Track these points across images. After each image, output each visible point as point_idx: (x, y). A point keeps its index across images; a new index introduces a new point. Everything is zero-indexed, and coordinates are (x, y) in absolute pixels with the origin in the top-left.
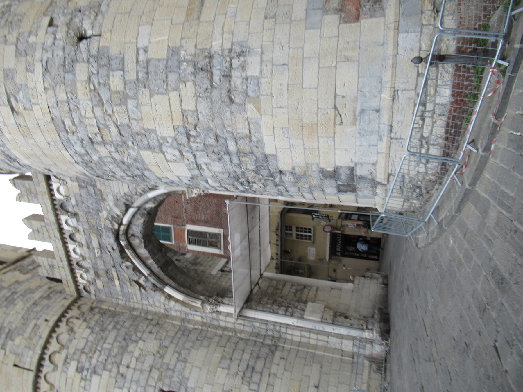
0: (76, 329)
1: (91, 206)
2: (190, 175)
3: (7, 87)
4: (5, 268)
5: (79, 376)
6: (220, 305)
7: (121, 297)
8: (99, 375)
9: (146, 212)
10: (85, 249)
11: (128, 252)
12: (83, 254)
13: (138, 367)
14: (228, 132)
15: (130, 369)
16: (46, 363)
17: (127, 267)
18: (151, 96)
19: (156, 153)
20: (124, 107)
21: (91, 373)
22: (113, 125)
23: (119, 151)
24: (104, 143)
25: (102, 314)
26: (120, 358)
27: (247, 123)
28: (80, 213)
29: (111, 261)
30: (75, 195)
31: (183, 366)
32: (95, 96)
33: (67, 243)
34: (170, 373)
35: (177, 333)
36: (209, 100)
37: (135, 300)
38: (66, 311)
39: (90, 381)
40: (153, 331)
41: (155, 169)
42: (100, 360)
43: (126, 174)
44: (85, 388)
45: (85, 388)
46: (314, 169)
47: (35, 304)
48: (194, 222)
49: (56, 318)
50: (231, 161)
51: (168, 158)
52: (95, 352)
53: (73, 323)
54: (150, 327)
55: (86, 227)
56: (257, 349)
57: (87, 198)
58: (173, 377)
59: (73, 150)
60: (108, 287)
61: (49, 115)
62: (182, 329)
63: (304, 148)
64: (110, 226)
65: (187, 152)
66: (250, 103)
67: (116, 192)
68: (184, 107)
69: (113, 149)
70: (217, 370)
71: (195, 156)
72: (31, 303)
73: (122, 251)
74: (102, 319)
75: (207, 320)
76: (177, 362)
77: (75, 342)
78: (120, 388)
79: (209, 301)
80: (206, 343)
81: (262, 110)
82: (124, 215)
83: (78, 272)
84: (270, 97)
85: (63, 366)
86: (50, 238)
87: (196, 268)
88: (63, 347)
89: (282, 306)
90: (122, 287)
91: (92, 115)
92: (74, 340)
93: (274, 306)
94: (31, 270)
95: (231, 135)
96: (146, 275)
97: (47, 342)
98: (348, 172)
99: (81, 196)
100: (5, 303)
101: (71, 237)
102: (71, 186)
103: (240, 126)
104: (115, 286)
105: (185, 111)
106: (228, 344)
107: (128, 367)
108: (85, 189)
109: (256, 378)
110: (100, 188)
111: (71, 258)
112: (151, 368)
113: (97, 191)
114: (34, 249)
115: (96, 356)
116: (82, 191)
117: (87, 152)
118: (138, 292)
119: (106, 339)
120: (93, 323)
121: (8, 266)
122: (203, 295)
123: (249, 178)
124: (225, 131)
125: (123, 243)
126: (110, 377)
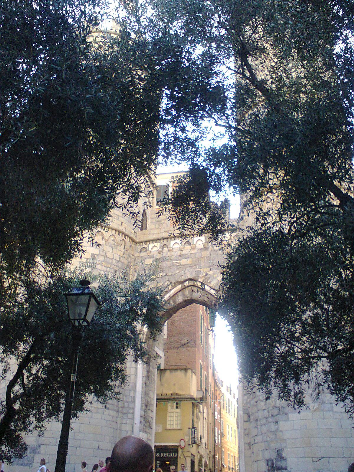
0: (119, 247)
10: (179, 253)
12: (174, 250)
29: (171, 273)
38: (128, 236)
46: (282, 444)
49: (124, 231)
55: (197, 256)
63: (295, 439)
73: (180, 283)
77: (110, 249)
83: (158, 244)
88: (107, 241)
98: (284, 466)
120: (123, 260)
125: (187, 283)
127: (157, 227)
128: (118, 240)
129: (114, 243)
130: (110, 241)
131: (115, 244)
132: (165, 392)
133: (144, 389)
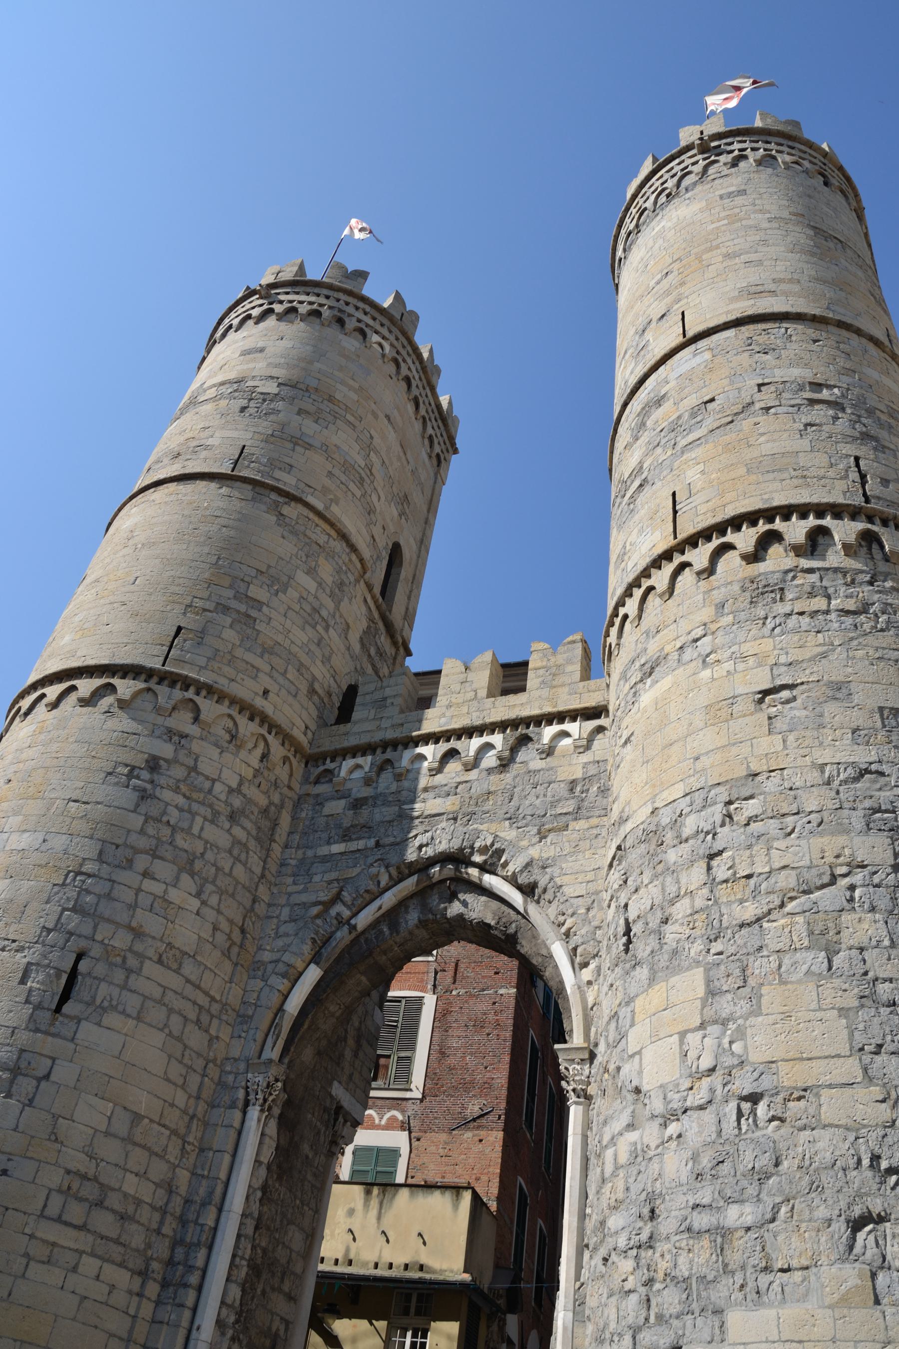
0: (243, 754)
1: (527, 802)
2: (645, 1088)
3: (811, 685)
4: (376, 602)
5: (139, 760)
6: (262, 1111)
7: (300, 852)
8: (137, 805)
9: (511, 930)
11: (410, 884)
13: (141, 896)
14: (776, 1209)
15: (141, 877)
16: (178, 694)
17: (375, 878)
18: (843, 1012)
19: (702, 1009)
20: (806, 943)
21: (145, 790)
22: (759, 912)
23: (696, 917)
24: (712, 883)
25: (265, 812)
26: (169, 856)
27: (805, 1263)
28: (508, 777)
29: (392, 839)
30: (552, 769)
31: (129, 1010)
32: (820, 875)
33: (437, 742)
34: (119, 976)
35: (207, 994)
36: (852, 1162)
37: (290, 889)
39: (127, 787)
40: (218, 934)
41: (657, 995)
42: (170, 809)
43: (634, 921)
44: (110, 774)
45: (110, 774)
47: (301, 668)
48: (441, 1017)
49: (269, 710)
50: (696, 1206)
51: (689, 1036)
52: (188, 798)
53: (255, 746)
54: (224, 926)
55: (477, 789)
56: (145, 1214)
57: (545, 796)
58: (111, 983)
59: (689, 809)
60: (327, 823)
61: (765, 768)
62: (215, 1008)
64: (477, 845)
65: (712, 1091)
66: (860, 1276)
67: (564, 865)
68: (825, 1093)
69: (699, 903)
70: (109, 1101)
71: (701, 1108)
72: (304, 659)
74: (256, 811)
75: (230, 1073)
76: (142, 995)
77: (215, 753)
78: (101, 853)
79: (277, 1080)
80: (176, 1071)
81: (845, 1311)
82: (505, 878)
83: (366, 761)
84: (881, 1337)
85: (167, 728)
86: (449, 706)
87: (351, 1042)
89: (243, 1290)
90: (325, 859)
91: (777, 865)
92: (219, 751)
93: (245, 1269)
94: (368, 651)
95: (768, 1216)
96: (353, 922)
97: (219, 696)
99: (550, 783)
100: (308, 608)
101: (452, 754)
102: (574, 762)
103: (795, 1241)
104: (329, 843)
105: (818, 1095)
106: (168, 1132)
107: (146, 874)
108: (566, 794)
109: (76, 1212)
110: (570, 827)
111: (400, 747)
112: (138, 933)
113: (564, 819)
114: (409, 653)
115: (180, 800)
116: (562, 785)
117: (686, 840)
118: (313, 898)
119: (212, 822)
120: (251, 791)
121: (378, 607)
122: (290, 1066)
123: (650, 1252)
124: (778, 1200)
126: (129, 831)
127: (371, 717)
128: (241, 730)
129: (227, 737)
130: (219, 731)
131: (230, 742)
132: (387, 1258)
133: (255, 1208)
